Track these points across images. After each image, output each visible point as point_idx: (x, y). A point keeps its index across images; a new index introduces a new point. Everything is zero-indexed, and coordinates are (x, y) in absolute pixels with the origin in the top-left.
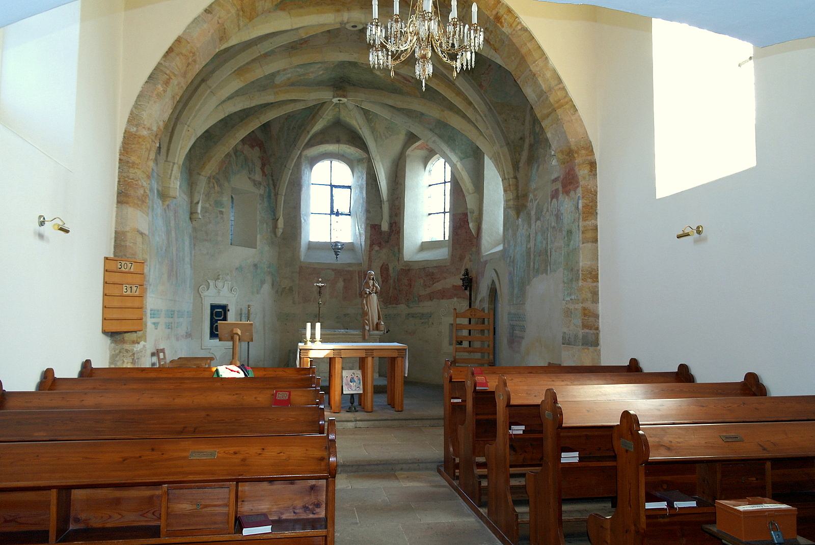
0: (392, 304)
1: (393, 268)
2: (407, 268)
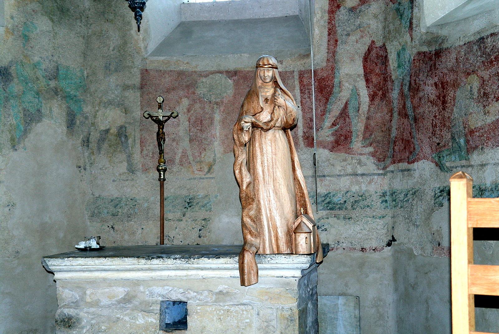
0: (400, 161)
1: (399, 55)
2: (433, 49)
